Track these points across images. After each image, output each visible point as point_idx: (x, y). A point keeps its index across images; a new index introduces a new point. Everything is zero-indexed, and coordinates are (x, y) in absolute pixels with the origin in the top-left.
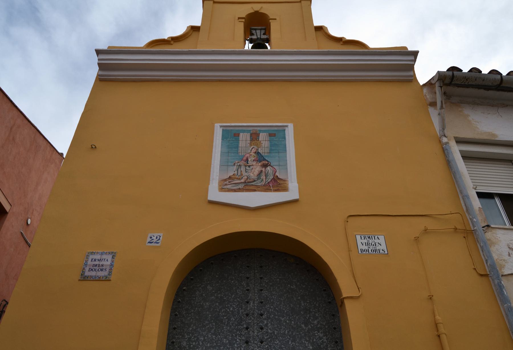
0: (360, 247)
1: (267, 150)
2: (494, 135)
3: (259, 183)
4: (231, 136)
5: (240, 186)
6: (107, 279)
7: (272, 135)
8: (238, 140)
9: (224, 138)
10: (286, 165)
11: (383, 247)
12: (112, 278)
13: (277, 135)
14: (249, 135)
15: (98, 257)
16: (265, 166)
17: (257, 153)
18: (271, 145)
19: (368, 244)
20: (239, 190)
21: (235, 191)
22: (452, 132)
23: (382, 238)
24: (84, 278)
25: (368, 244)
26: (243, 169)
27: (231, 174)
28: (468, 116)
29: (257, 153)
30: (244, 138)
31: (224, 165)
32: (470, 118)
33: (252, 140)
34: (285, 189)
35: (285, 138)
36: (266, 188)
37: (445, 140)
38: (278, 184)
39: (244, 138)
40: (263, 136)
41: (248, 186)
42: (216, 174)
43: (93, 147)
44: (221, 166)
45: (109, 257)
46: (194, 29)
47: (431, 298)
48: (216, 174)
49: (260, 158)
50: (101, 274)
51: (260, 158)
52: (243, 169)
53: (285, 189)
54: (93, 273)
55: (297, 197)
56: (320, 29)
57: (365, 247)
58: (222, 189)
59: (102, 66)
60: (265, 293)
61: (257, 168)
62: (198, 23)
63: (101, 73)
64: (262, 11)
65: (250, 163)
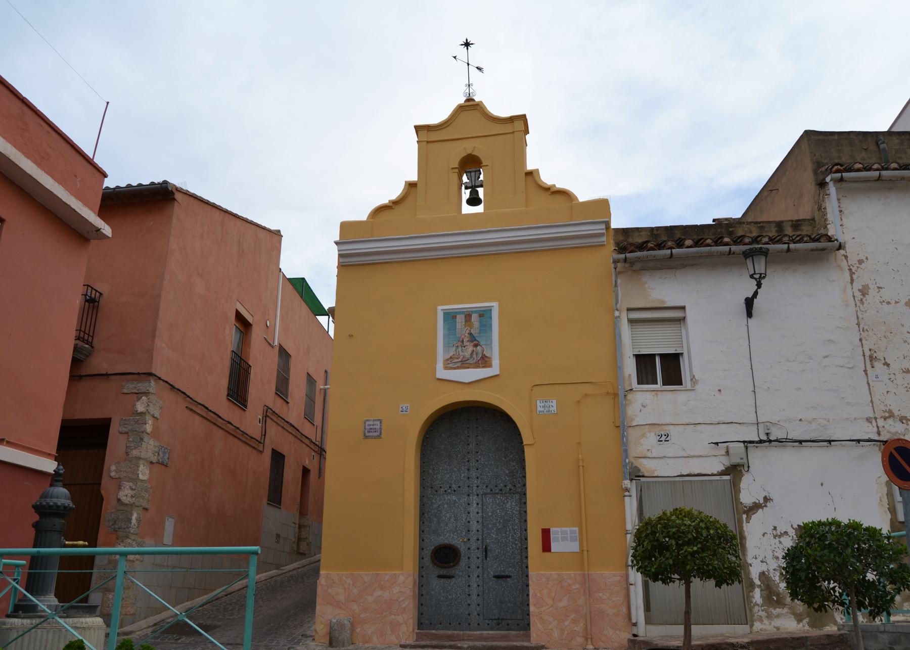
0: (539, 409)
1: (477, 331)
2: (664, 302)
3: (471, 361)
4: (450, 317)
5: (459, 365)
6: (379, 437)
7: (481, 316)
8: (455, 322)
9: (445, 320)
10: (491, 344)
11: (555, 408)
12: (383, 435)
13: (485, 314)
14: (463, 316)
15: (371, 423)
16: (476, 346)
17: (470, 334)
18: (481, 326)
19: (544, 407)
20: (458, 368)
21: (455, 368)
22: (624, 304)
23: (554, 401)
24: (366, 437)
25: (544, 407)
26: (460, 349)
27: (451, 354)
28: (645, 283)
29: (470, 334)
30: (460, 319)
31: (447, 346)
32: (647, 286)
33: (466, 321)
34: (490, 366)
35: (491, 318)
36: (477, 365)
37: (617, 314)
38: (484, 362)
39: (460, 319)
40: (475, 317)
41: (464, 364)
42: (441, 356)
43: (351, 336)
44: (444, 347)
45: (378, 423)
46: (411, 185)
47: (579, 443)
48: (441, 356)
49: (472, 338)
50: (375, 434)
51: (472, 338)
52: (460, 349)
53: (490, 366)
54: (371, 434)
55: (498, 373)
56: (531, 174)
57: (542, 409)
58: (446, 368)
59: (340, 256)
60: (480, 438)
61: (470, 348)
62: (414, 178)
63: (341, 260)
64: (475, 153)
65: (465, 343)
